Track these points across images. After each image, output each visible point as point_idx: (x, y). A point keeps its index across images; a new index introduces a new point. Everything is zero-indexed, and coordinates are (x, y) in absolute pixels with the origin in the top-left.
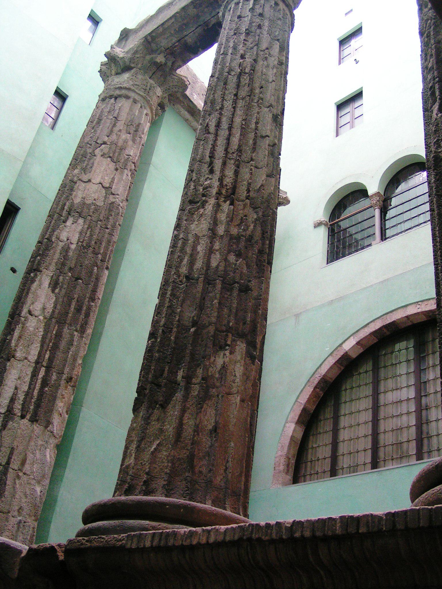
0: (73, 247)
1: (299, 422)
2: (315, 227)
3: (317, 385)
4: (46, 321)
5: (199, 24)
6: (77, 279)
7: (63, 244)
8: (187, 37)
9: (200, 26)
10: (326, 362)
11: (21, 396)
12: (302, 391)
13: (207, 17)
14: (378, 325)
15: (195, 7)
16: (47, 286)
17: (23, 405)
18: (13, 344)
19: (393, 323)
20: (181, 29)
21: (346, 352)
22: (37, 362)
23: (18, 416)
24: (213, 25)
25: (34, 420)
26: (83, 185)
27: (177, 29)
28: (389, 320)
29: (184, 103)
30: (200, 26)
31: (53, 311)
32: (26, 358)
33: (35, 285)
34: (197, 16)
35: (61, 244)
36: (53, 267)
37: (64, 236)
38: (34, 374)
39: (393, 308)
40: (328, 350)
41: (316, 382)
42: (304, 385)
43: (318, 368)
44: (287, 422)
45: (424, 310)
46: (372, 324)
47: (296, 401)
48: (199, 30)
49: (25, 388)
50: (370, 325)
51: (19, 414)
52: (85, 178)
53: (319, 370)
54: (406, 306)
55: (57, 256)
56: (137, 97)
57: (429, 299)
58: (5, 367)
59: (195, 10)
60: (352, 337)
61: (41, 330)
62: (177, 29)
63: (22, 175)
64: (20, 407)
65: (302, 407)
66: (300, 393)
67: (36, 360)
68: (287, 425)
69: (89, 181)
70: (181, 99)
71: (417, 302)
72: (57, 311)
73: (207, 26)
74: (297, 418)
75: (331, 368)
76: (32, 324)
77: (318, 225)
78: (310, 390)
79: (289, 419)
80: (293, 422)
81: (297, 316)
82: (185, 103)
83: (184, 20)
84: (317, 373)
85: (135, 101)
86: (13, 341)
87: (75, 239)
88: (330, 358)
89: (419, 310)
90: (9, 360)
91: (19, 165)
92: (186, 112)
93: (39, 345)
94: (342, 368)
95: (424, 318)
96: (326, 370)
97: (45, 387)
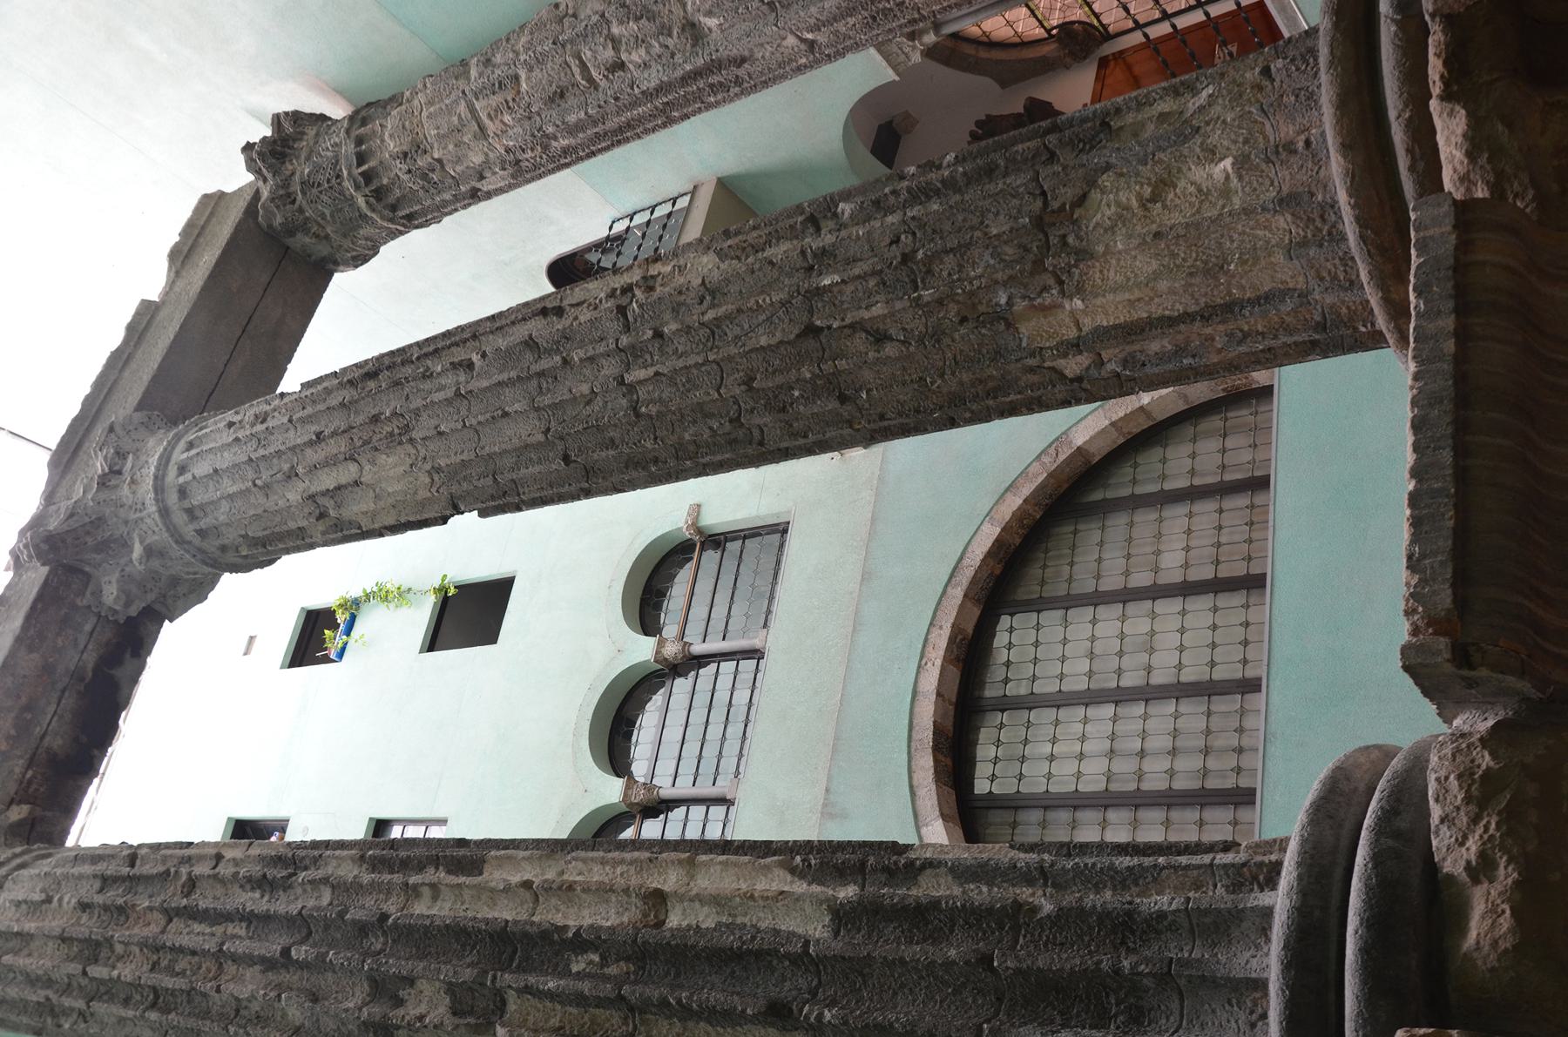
5: (60, 686)
8: (48, 739)
9: (63, 691)
13: (71, 659)
14: (926, 762)
15: (31, 649)
19: (938, 731)
20: (23, 728)
24: (96, 670)
27: (13, 732)
28: (926, 734)
30: (63, 691)
34: (47, 669)
39: (906, 722)
45: (942, 653)
46: (915, 776)
48: (69, 701)
50: (915, 783)
54: (915, 693)
57: (926, 640)
59: (35, 656)
62: (13, 732)
71: (919, 666)
73: (82, 679)
83: (19, 697)
89: (939, 662)
95: (955, 673)
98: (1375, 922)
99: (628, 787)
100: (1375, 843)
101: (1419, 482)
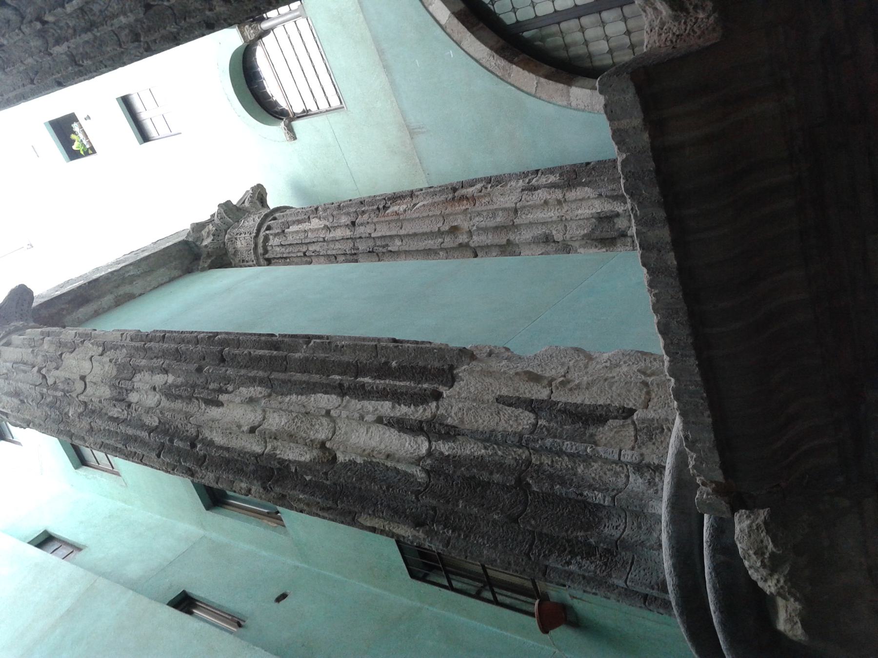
0: (171, 379)
1: (569, 83)
2: (295, 138)
3: (507, 59)
4: (274, 395)
6: (223, 360)
7: (163, 398)
10: (471, 50)
11: (403, 410)
12: (519, 89)
16: (221, 410)
17: (416, 405)
18: (307, 457)
21: (453, 13)
22: (341, 390)
23: (437, 408)
25: (449, 377)
26: (89, 390)
29: (63, 309)
31: (261, 382)
32: (328, 413)
33: (219, 439)
35: (165, 403)
36: (192, 408)
37: (152, 400)
38: (364, 393)
40: (453, 52)
41: (502, 62)
42: (509, 87)
43: (481, 64)
44: (569, 106)
47: (534, 96)
49: (386, 407)
51: (434, 404)
52: (79, 386)
53: (483, 61)
55: (179, 405)
56: (4, 341)
58: (345, 465)
60: (430, 8)
61: (287, 399)
63: (134, 586)
64: (421, 409)
65: (542, 80)
66: (522, 91)
67: (338, 395)
68: (574, 104)
69: (83, 378)
70: (54, 311)
72: (261, 374)
74: (561, 86)
75: (479, 38)
76: (276, 421)
77: (290, 130)
78: (518, 74)
79: (565, 103)
80: (569, 92)
81: (412, 132)
82: (63, 306)
84: (488, 66)
85: (8, 344)
86: (303, 459)
87: (159, 379)
88: (465, 45)
90: (335, 458)
91: (102, 582)
92: (81, 310)
93: (313, 397)
94: (481, 25)
96: (483, 47)
97: (390, 368)
98: (721, 610)
99: (242, 33)
100: (713, 557)
101: (677, 380)
